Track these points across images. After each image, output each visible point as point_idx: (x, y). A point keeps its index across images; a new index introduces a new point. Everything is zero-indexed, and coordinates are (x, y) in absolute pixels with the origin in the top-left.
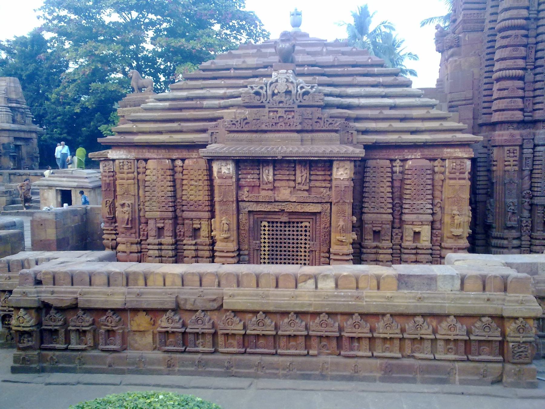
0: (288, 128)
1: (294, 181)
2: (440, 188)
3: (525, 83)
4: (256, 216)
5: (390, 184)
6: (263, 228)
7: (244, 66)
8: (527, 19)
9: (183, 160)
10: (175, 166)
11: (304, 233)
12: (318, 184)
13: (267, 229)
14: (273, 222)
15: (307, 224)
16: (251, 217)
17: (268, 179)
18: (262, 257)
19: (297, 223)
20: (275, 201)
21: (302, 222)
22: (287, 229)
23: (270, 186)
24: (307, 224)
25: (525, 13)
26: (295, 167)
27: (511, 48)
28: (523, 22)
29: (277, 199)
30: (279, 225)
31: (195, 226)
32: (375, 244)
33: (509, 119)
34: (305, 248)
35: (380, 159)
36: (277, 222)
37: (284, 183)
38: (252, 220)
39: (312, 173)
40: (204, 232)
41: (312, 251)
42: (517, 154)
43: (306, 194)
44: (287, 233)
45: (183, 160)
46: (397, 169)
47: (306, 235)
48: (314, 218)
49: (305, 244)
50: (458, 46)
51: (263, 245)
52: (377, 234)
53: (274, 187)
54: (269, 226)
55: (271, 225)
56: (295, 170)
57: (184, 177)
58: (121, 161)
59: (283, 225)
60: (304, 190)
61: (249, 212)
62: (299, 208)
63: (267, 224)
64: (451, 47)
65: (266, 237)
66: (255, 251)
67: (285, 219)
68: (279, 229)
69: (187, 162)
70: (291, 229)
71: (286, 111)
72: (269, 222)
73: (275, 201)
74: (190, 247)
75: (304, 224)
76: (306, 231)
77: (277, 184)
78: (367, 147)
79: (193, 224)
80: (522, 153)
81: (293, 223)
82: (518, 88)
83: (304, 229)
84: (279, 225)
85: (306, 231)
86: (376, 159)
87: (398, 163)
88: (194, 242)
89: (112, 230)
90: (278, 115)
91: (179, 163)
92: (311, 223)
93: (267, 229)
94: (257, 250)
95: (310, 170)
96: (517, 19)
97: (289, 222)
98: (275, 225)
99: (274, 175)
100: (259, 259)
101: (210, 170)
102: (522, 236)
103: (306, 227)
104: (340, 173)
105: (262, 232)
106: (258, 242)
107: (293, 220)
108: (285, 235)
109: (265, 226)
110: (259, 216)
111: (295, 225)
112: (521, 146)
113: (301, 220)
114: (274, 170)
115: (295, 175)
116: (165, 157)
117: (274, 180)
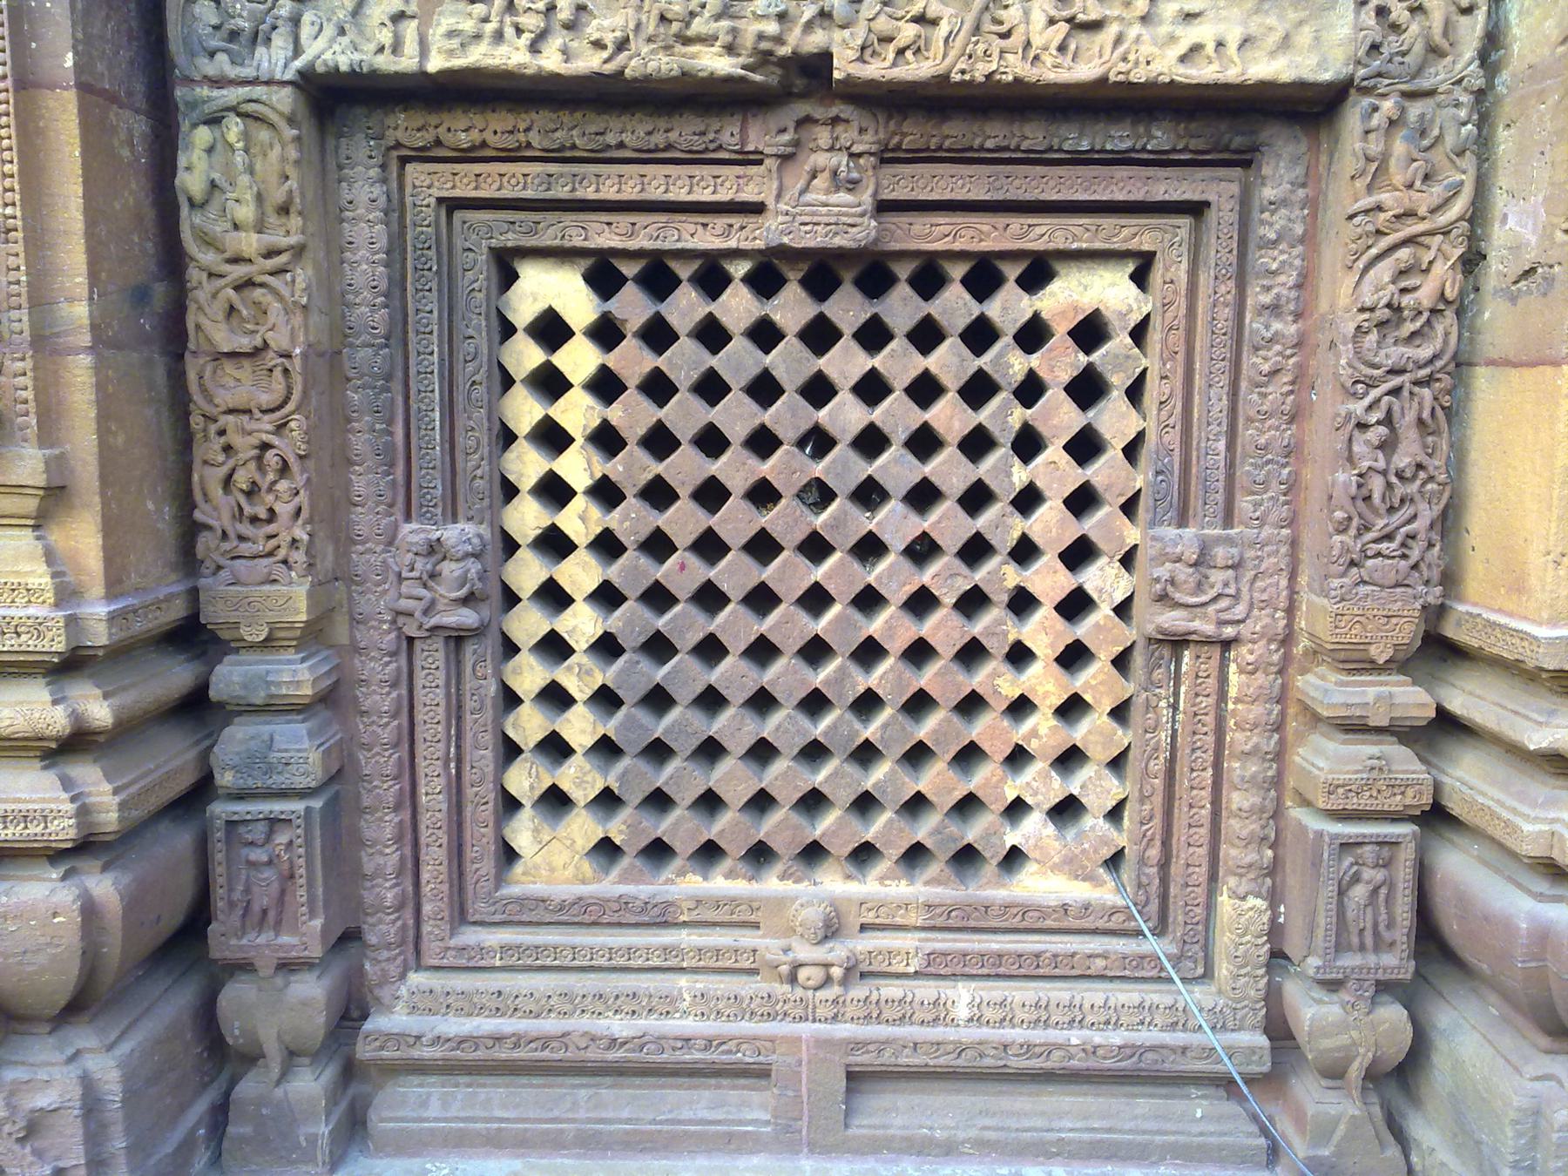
4: (429, 183)
6: (526, 356)
11: (1059, 417)
13: (579, 359)
14: (658, 277)
15: (1107, 290)
18: (529, 725)
21: (1037, 273)
24: (1107, 290)
30: (738, 306)
38: (367, 236)
41: (1177, 643)
48: (1218, 189)
51: (528, 572)
54: (606, 333)
55: (633, 306)
59: (792, 308)
63: (576, 301)
65: (577, 467)
66: (432, 659)
67: (816, 197)
68: (739, 361)
72: (603, 278)
75: (1065, 297)
83: (1060, 362)
84: (738, 306)
85: (1087, 389)
92: (1171, 270)
93: (579, 359)
94: (457, 639)
97: (875, 275)
100: (483, 756)
103: (1090, 332)
106: (455, 534)
109: (551, 330)
111: (955, 305)
113: (1044, 234)
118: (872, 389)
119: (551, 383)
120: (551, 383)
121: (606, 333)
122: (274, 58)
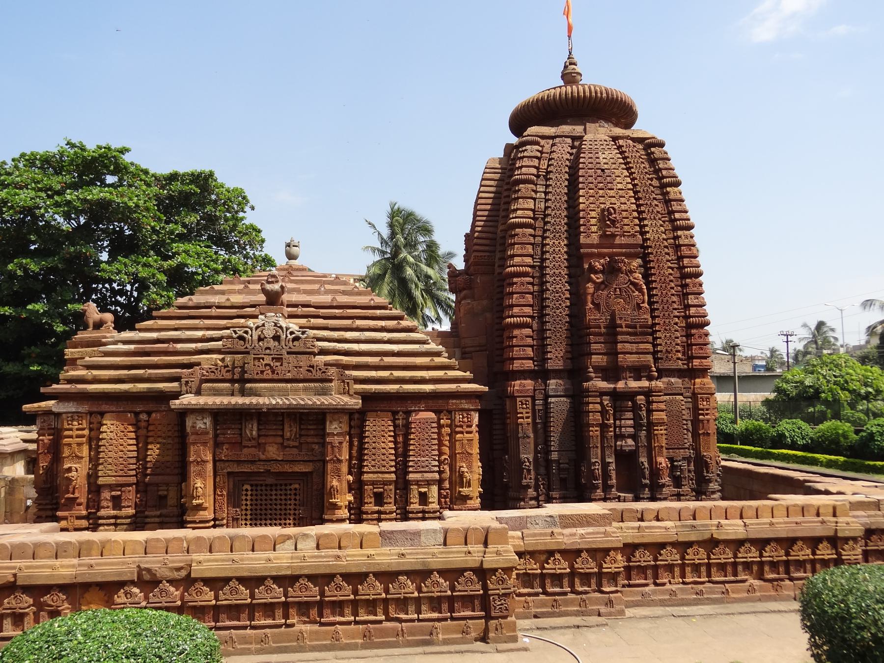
0: (275, 377)
1: (282, 436)
2: (447, 443)
3: (533, 331)
4: (237, 479)
5: (392, 439)
6: (244, 493)
7: (228, 304)
9: (149, 414)
10: (138, 421)
11: (293, 497)
12: (309, 440)
14: (257, 485)
15: (297, 486)
16: (231, 480)
17: (251, 434)
19: (286, 485)
20: (260, 460)
21: (291, 485)
22: (274, 492)
23: (253, 443)
25: (529, 260)
26: (283, 421)
28: (529, 269)
29: (263, 457)
30: (263, 488)
31: (160, 493)
32: (377, 508)
34: (295, 514)
35: (381, 411)
36: (261, 485)
37: (271, 440)
39: (302, 427)
40: (171, 501)
42: (530, 406)
43: (295, 451)
44: (274, 497)
45: (149, 414)
46: (400, 422)
47: (295, 500)
49: (295, 510)
50: (470, 288)
52: (379, 499)
53: (259, 444)
55: (254, 488)
56: (283, 425)
57: (150, 434)
58: (70, 415)
59: (268, 488)
60: (294, 447)
61: (229, 473)
62: (287, 468)
63: (249, 488)
64: (464, 289)
65: (248, 503)
67: (270, 481)
69: (154, 415)
70: (279, 492)
71: (273, 359)
72: (252, 485)
73: (260, 460)
74: (152, 520)
75: (293, 487)
76: (295, 494)
77: (262, 440)
78: (366, 397)
79: (158, 491)
80: (534, 405)
81: (281, 485)
84: (263, 488)
86: (377, 411)
87: (401, 416)
88: (158, 513)
89: (46, 504)
90: (264, 363)
91: (144, 417)
95: (301, 424)
96: (522, 266)
97: (276, 485)
98: (259, 488)
99: (259, 430)
101: (183, 425)
102: (539, 495)
103: (296, 489)
104: (333, 427)
105: (244, 497)
107: (281, 482)
108: (271, 500)
109: (247, 490)
110: (240, 479)
111: (283, 487)
112: (534, 398)
114: (259, 424)
115: (283, 430)
116: (127, 409)
117: (259, 436)
118: (276, 495)
119: (246, 495)
120: (246, 495)
121: (252, 490)
122: (225, 471)
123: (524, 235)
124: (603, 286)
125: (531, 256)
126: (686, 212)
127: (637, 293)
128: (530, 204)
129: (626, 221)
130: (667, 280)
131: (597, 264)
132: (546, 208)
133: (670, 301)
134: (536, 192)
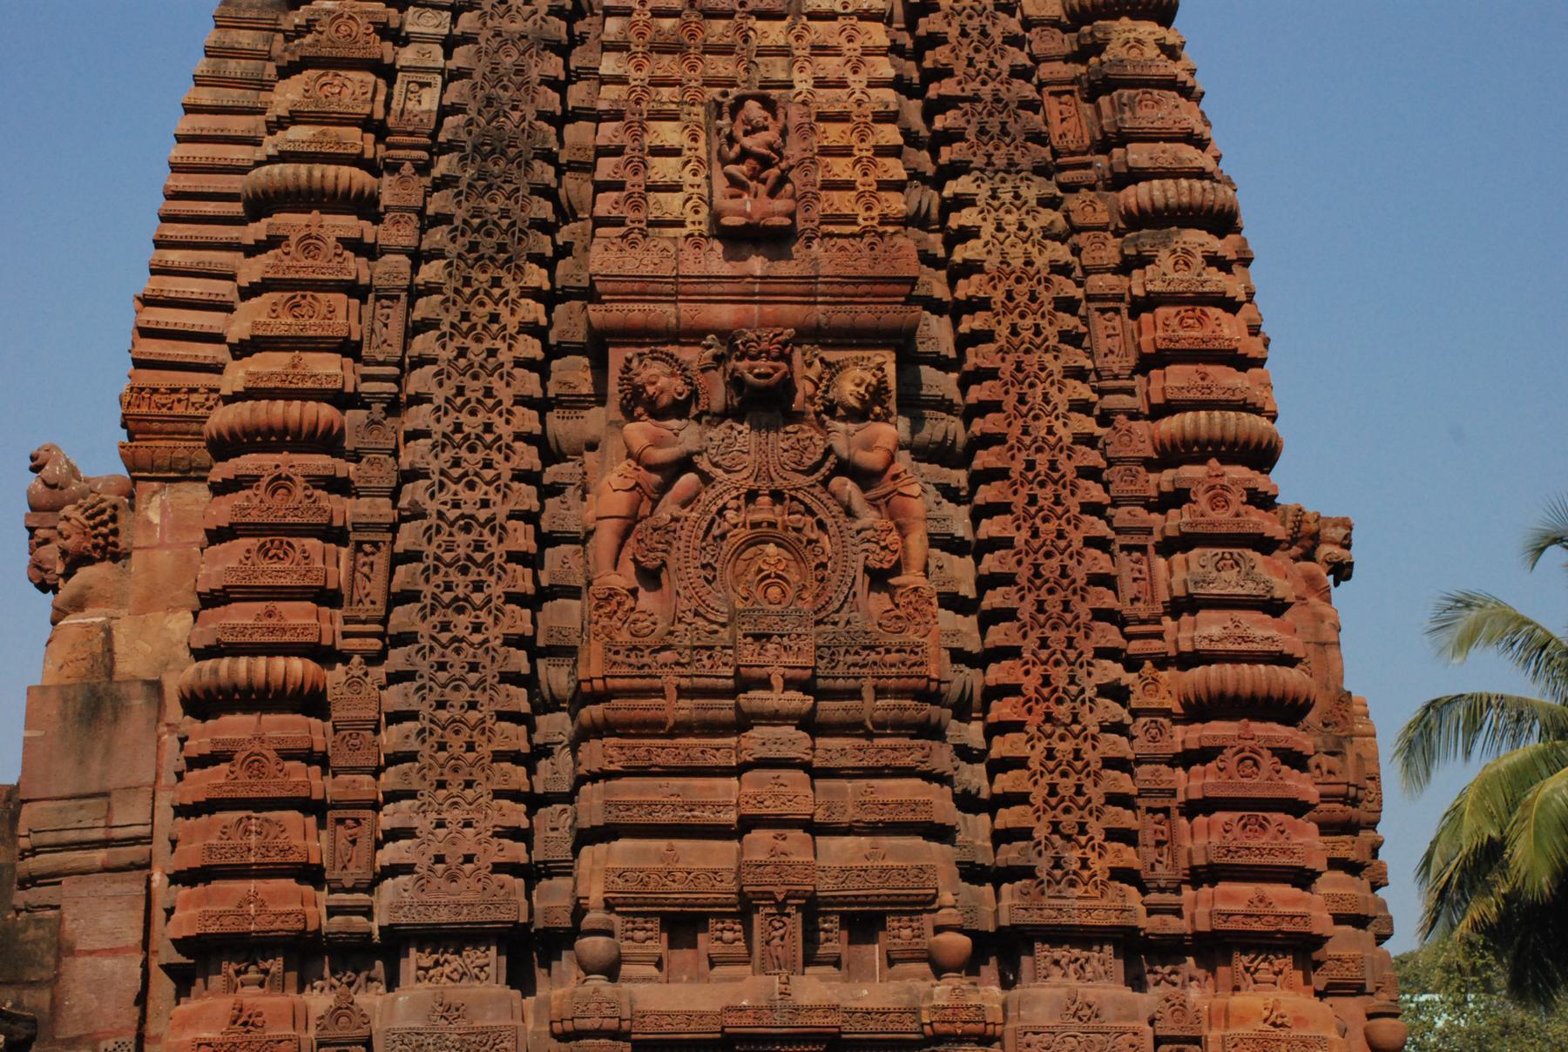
8: (343, 400)
27: (252, 543)
33: (230, 926)
82: (287, 755)
123: (310, 244)
124: (688, 479)
125: (349, 348)
126: (1201, 143)
127: (869, 517)
128: (354, 91)
129: (841, 168)
130: (1067, 467)
131: (656, 368)
132: (444, 111)
133: (1079, 574)
134: (400, 38)
